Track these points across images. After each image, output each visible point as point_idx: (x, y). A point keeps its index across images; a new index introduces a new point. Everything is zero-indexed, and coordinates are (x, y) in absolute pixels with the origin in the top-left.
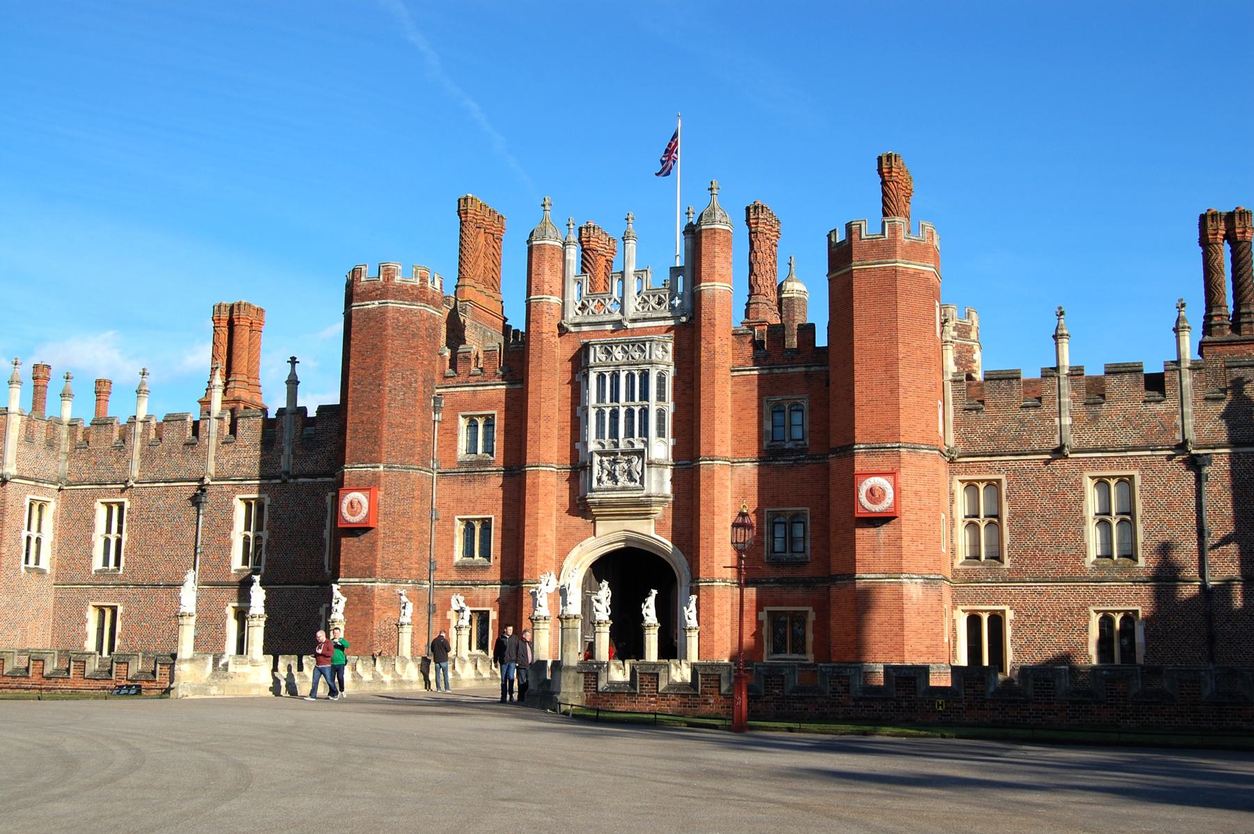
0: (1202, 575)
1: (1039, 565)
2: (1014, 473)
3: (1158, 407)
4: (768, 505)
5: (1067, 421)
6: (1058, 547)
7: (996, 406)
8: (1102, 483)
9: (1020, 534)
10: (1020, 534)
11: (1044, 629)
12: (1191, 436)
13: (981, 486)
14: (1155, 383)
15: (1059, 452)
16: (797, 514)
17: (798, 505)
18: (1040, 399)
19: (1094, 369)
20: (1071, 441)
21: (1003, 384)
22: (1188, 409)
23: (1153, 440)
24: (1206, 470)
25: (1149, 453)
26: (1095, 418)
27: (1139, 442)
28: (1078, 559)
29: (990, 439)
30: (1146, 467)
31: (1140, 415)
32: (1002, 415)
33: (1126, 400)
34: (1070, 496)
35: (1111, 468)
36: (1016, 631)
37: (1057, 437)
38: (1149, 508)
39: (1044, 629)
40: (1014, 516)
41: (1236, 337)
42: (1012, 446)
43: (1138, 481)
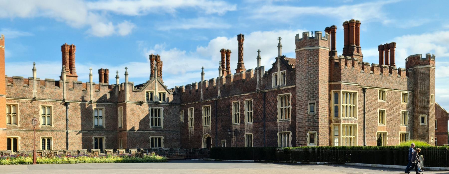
0: (67, 130)
5: (36, 91)
8: (44, 107)
12: (65, 98)
13: (12, 106)
14: (57, 84)
15: (34, 99)
18: (29, 85)
19: (43, 79)
20: (36, 96)
21: (19, 80)
22: (65, 92)
23: (56, 98)
24: (68, 106)
26: (43, 92)
27: (53, 98)
29: (15, 94)
30: (55, 104)
31: (53, 92)
32: (18, 88)
33: (50, 88)
34: (36, 110)
37: (33, 95)
38: (55, 114)
40: (21, 114)
41: (71, 75)
42: (21, 96)
43: (53, 108)
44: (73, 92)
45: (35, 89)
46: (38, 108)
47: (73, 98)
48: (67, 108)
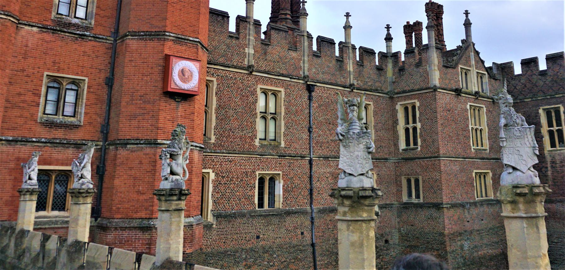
1: (231, 142)
2: (221, 79)
3: (294, 54)
4: (49, 70)
5: (252, 51)
6: (242, 131)
7: (214, 31)
9: (222, 120)
10: (222, 120)
11: (232, 186)
12: (307, 73)
16: (74, 82)
17: (77, 74)
22: (306, 59)
24: (313, 94)
25: (289, 79)
28: (252, 140)
35: (271, 85)
36: (215, 187)
39: (232, 186)
40: (219, 107)
42: (221, 60)
44: (319, 61)
45: (251, 47)
46: (254, 93)
47: (321, 77)
48: (310, 98)
